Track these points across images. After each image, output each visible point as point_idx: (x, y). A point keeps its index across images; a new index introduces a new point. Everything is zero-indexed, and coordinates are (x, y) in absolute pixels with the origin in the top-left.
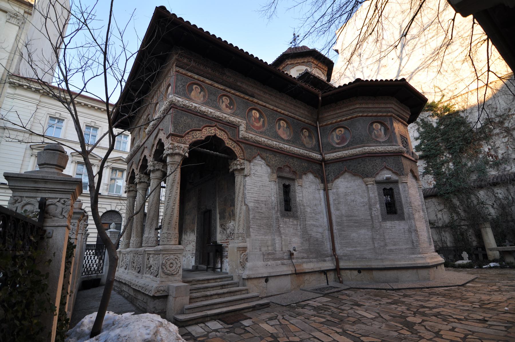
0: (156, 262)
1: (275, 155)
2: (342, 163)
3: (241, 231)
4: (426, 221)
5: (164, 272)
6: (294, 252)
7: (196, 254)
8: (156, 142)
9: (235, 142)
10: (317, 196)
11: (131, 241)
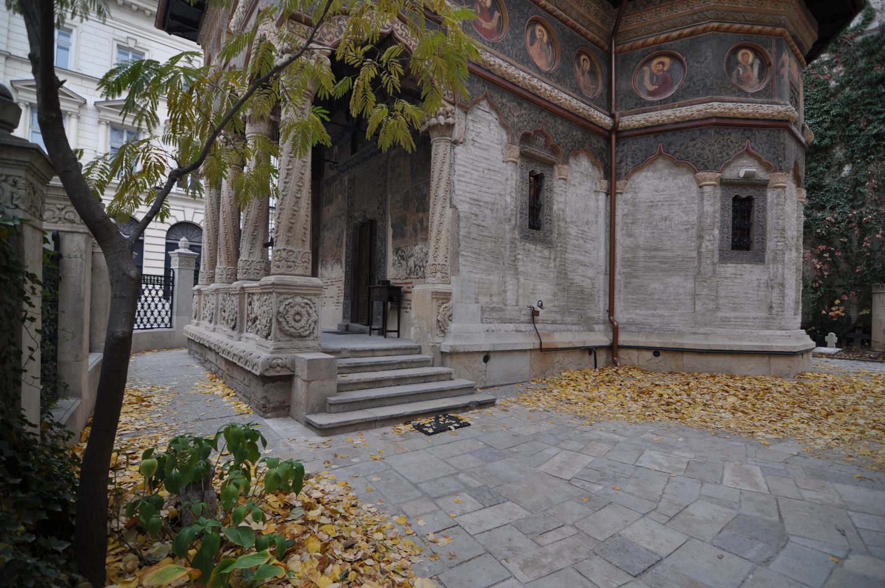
0: (265, 308)
1: (520, 104)
2: (655, 137)
3: (440, 260)
4: (797, 269)
5: (281, 330)
6: (539, 309)
10: (592, 204)
11: (217, 270)
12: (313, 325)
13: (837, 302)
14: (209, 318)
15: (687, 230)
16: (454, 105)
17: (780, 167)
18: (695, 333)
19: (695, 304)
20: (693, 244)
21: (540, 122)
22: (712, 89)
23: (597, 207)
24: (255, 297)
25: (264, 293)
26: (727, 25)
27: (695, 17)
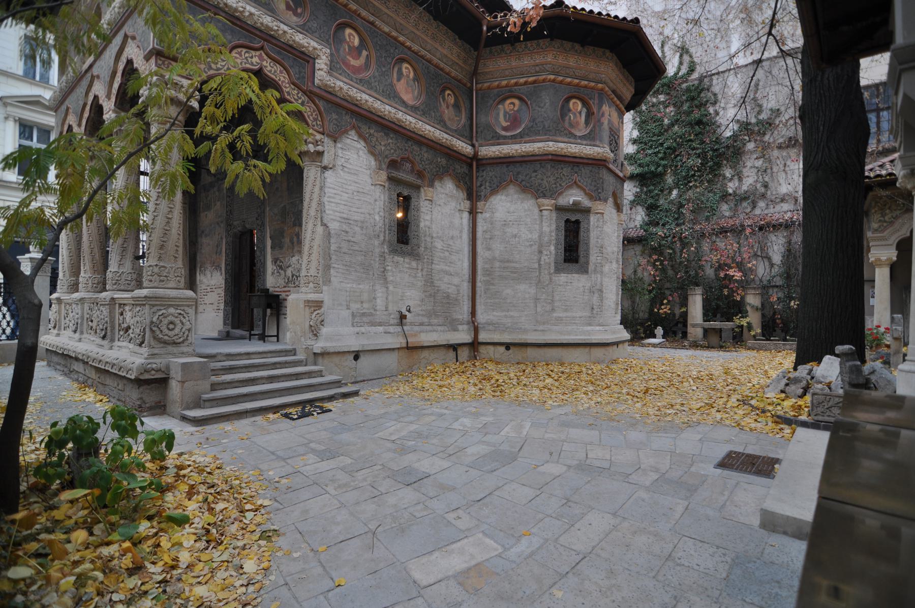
0: (138, 319)
1: (387, 135)
2: (507, 167)
3: (313, 272)
4: (618, 278)
5: (154, 338)
6: (407, 313)
7: (225, 310)
8: (121, 66)
9: (304, 92)
10: (457, 221)
11: (81, 279)
12: (187, 333)
13: (665, 301)
14: (74, 328)
15: (531, 246)
16: (323, 134)
21: (406, 150)
22: (550, 131)
23: (461, 224)
24: (127, 308)
25: (137, 305)
26: (561, 78)
27: (537, 69)
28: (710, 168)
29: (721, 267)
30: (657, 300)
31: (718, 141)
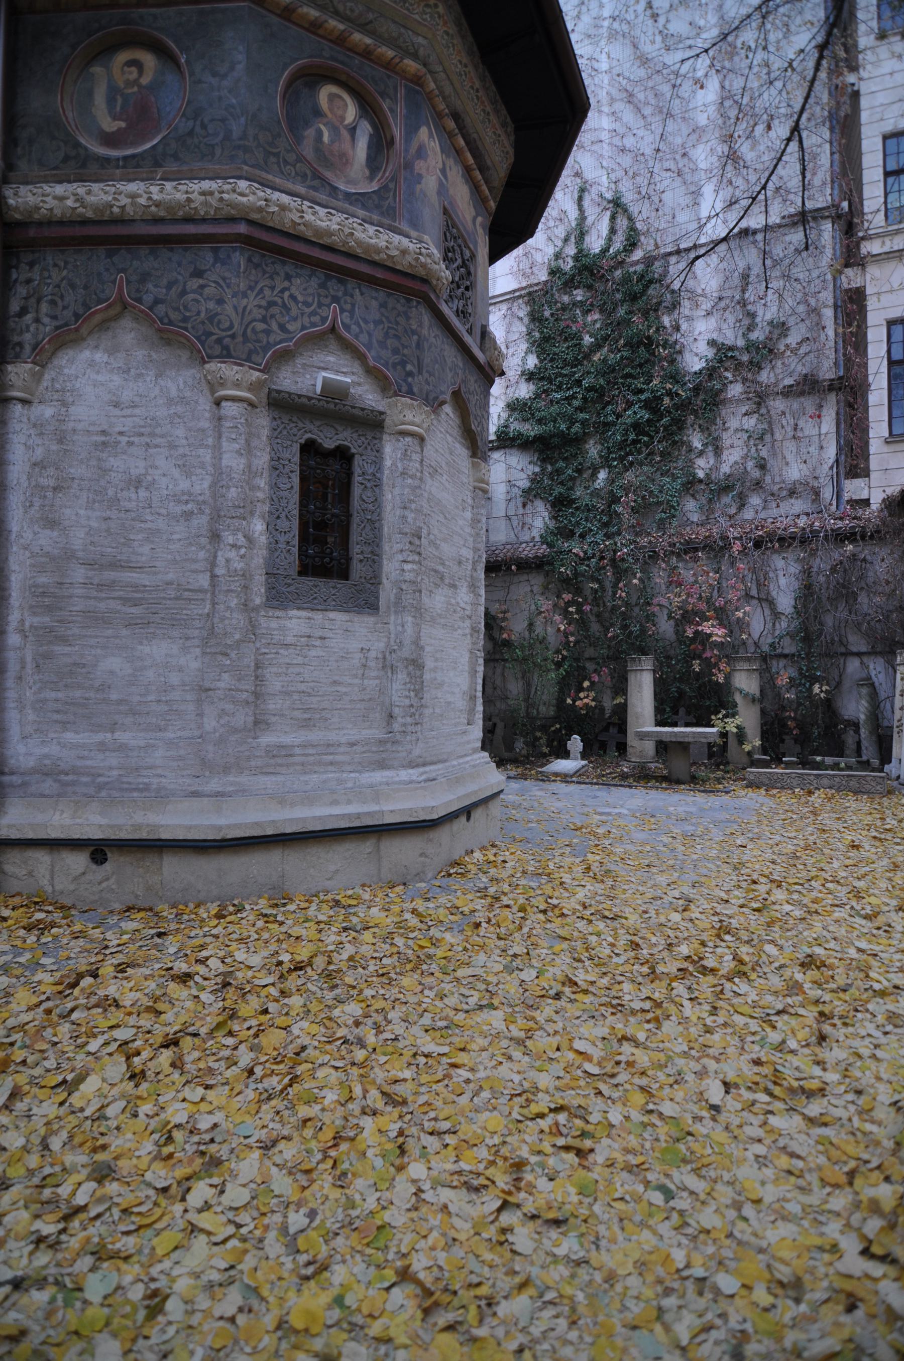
2: (110, 255)
13: (586, 684)
17: (410, 386)
18: (195, 794)
19: (201, 715)
20: (202, 555)
28: (666, 428)
29: (687, 616)
30: (571, 682)
31: (675, 377)
